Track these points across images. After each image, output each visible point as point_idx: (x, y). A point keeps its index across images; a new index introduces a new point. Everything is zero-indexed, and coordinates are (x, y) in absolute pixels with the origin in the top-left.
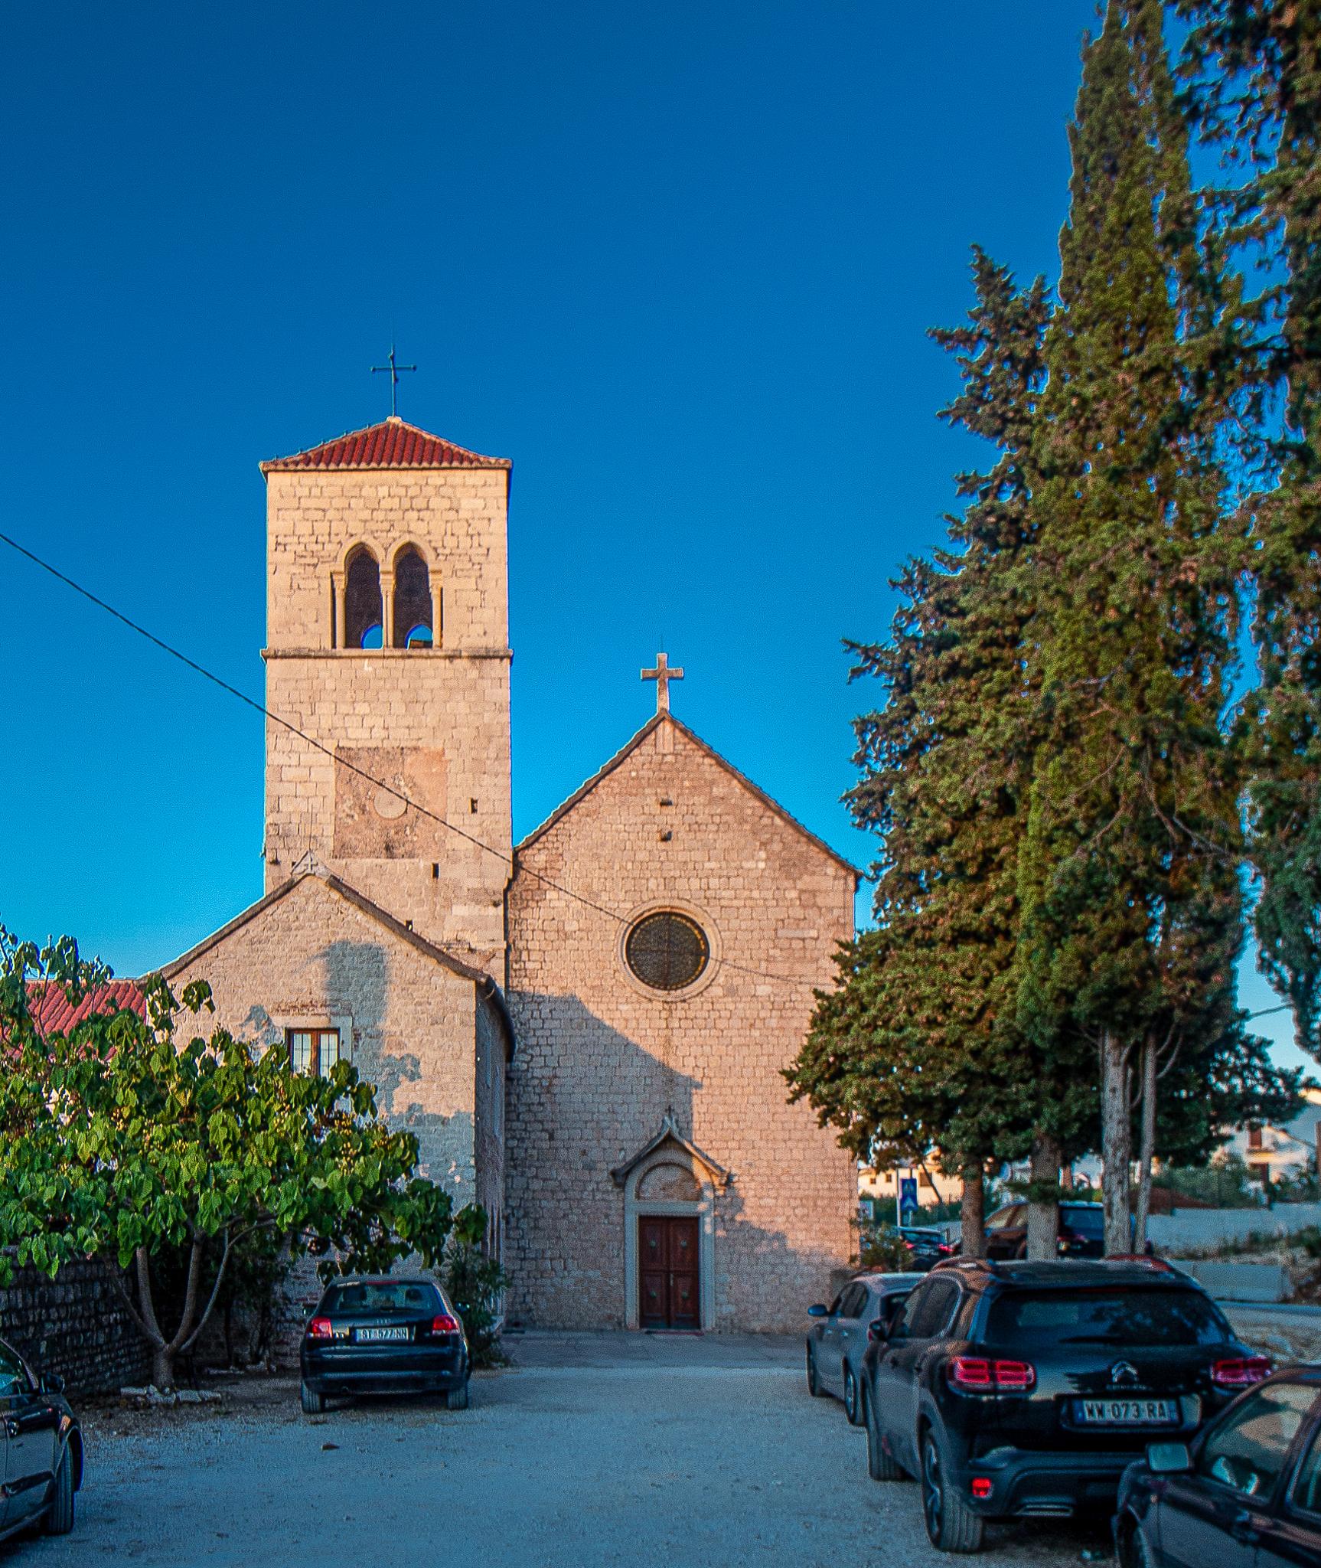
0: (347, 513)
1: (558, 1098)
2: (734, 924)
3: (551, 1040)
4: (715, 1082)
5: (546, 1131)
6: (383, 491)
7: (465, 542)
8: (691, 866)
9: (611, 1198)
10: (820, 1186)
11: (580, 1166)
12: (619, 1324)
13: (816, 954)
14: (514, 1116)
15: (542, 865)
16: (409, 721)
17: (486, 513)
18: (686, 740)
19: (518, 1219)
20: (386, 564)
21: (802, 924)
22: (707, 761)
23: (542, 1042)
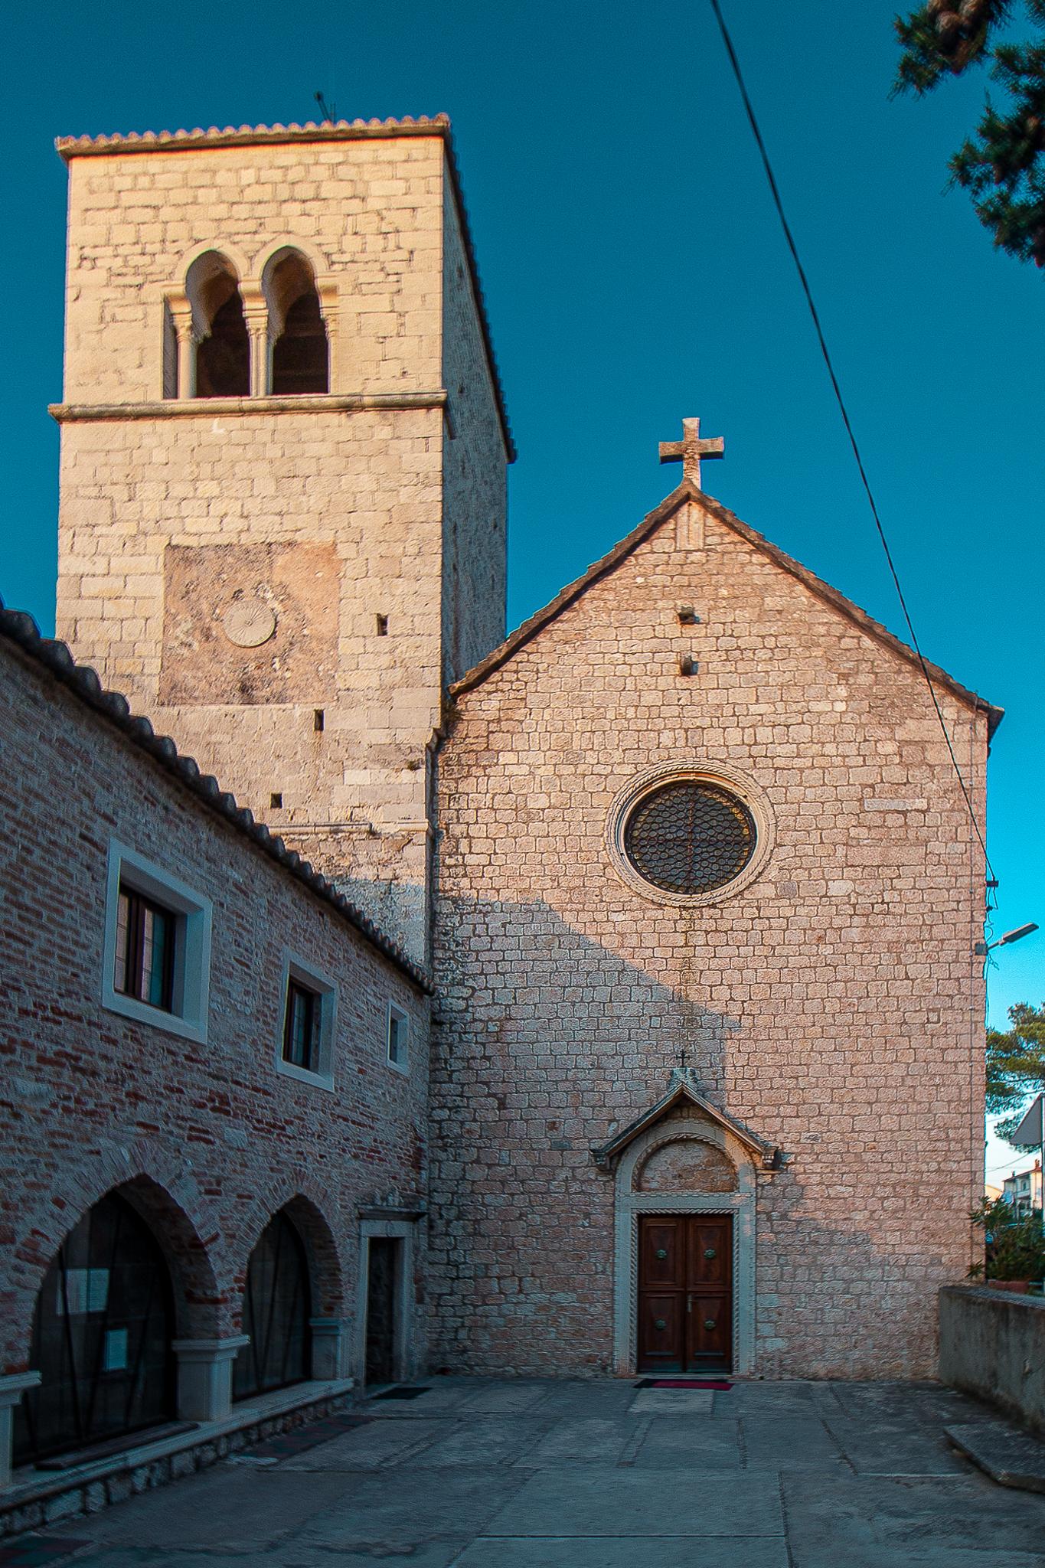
0: (191, 209)
1: (513, 1049)
2: (796, 793)
3: (504, 967)
4: (760, 1021)
5: (494, 1095)
6: (248, 176)
7: (375, 243)
8: (728, 710)
9: (594, 1189)
10: (924, 1167)
11: (546, 1145)
12: (604, 1369)
13: (924, 833)
14: (443, 1075)
15: (493, 715)
16: (280, 504)
17: (409, 201)
18: (724, 529)
19: (449, 1222)
20: (250, 279)
21: (903, 791)
22: (757, 558)
23: (489, 968)
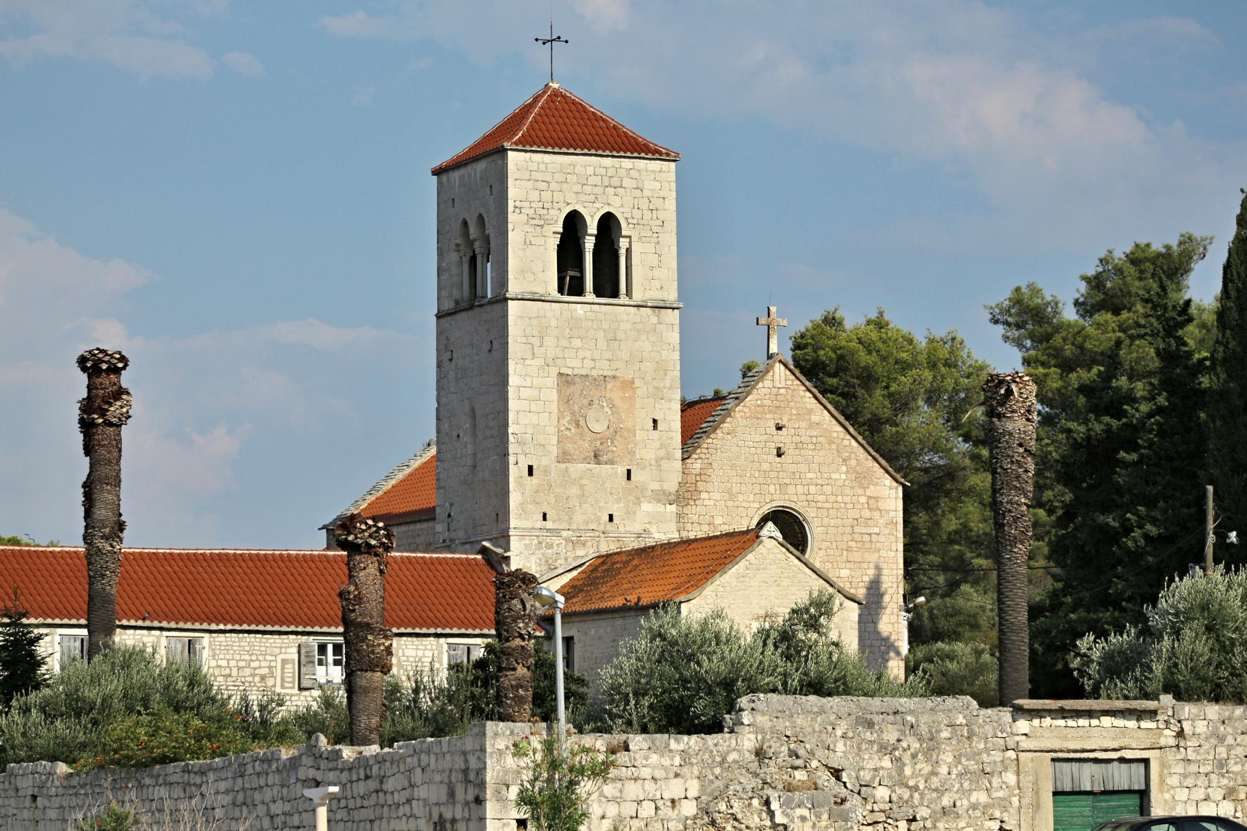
6: (590, 170)
7: (648, 215)
15: (698, 471)
17: (662, 194)
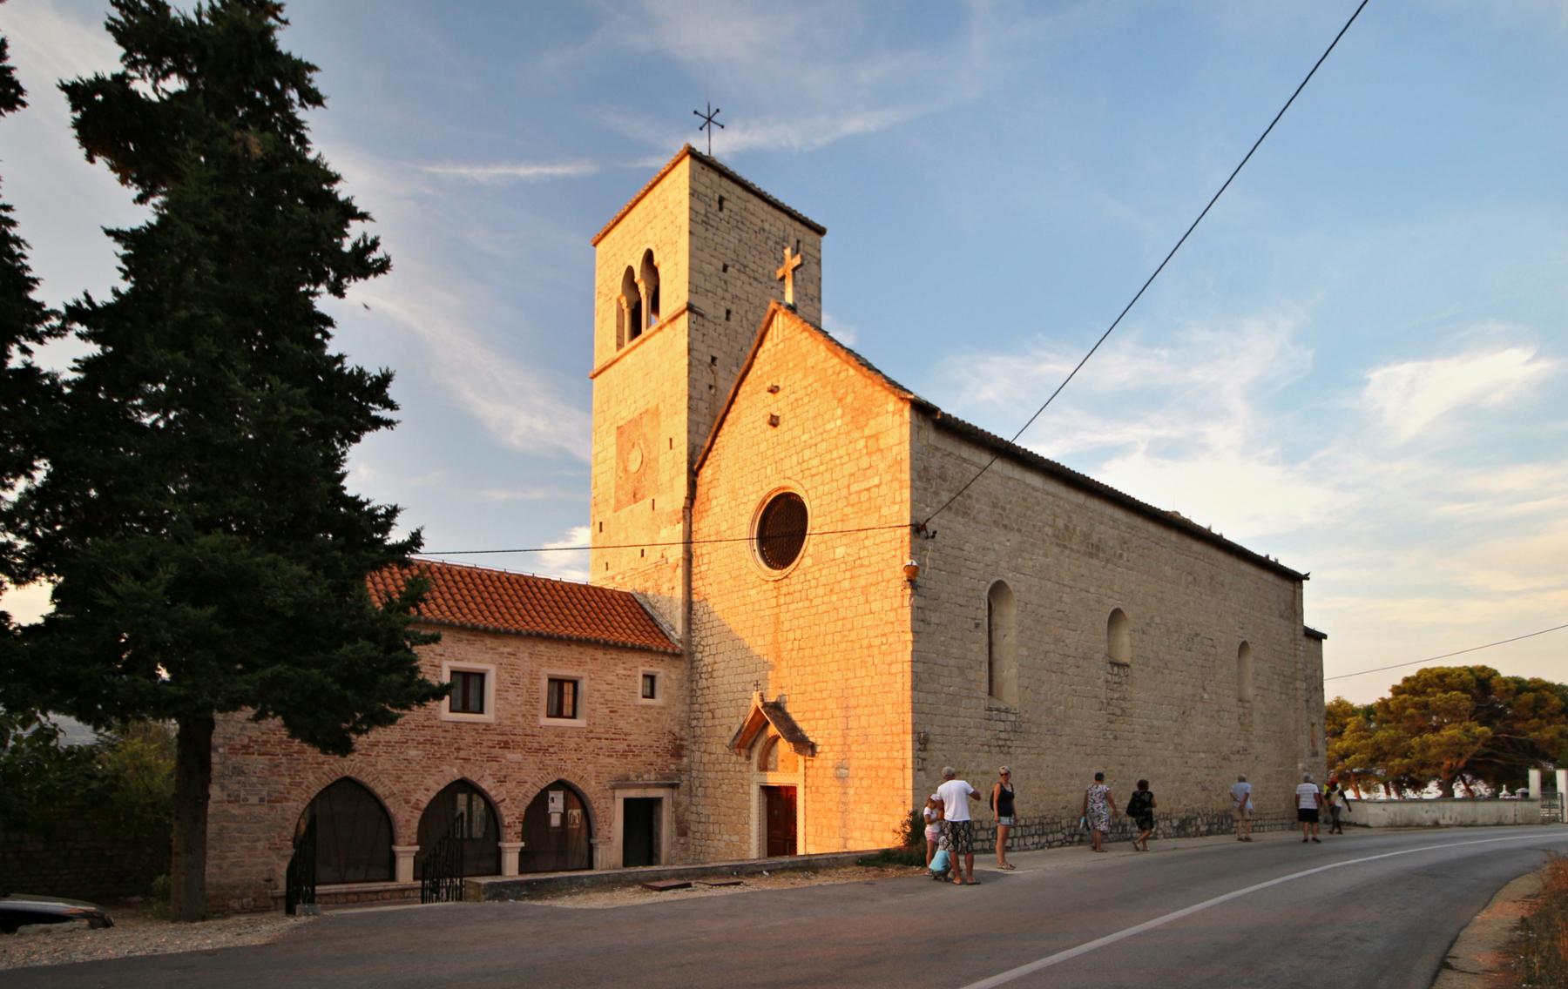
13: (879, 501)
